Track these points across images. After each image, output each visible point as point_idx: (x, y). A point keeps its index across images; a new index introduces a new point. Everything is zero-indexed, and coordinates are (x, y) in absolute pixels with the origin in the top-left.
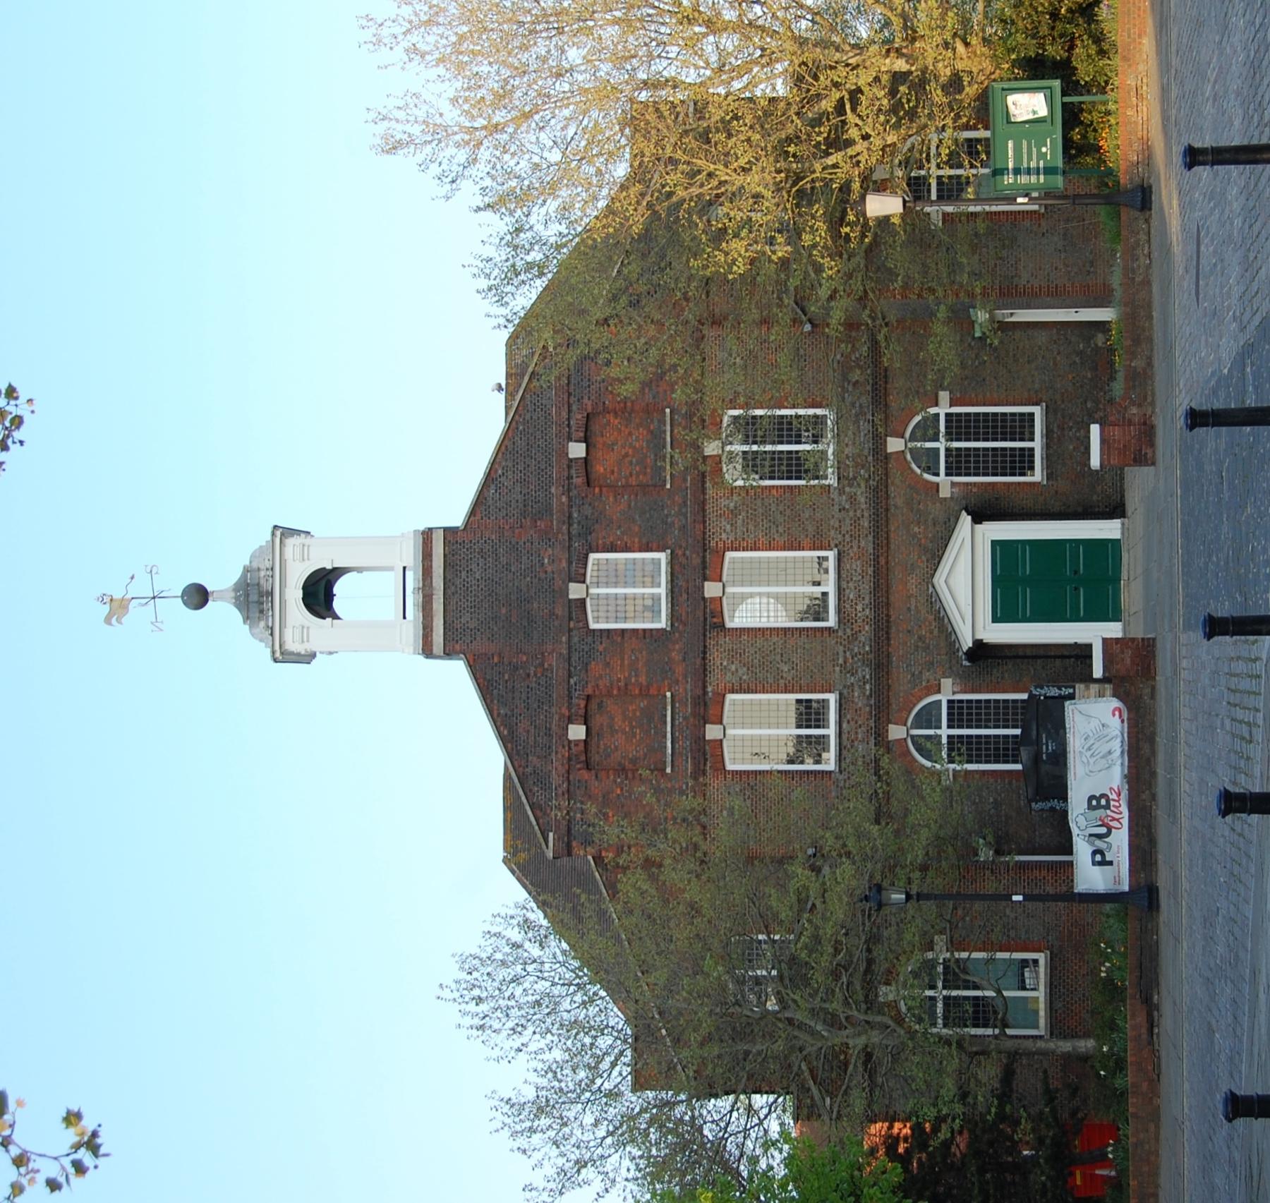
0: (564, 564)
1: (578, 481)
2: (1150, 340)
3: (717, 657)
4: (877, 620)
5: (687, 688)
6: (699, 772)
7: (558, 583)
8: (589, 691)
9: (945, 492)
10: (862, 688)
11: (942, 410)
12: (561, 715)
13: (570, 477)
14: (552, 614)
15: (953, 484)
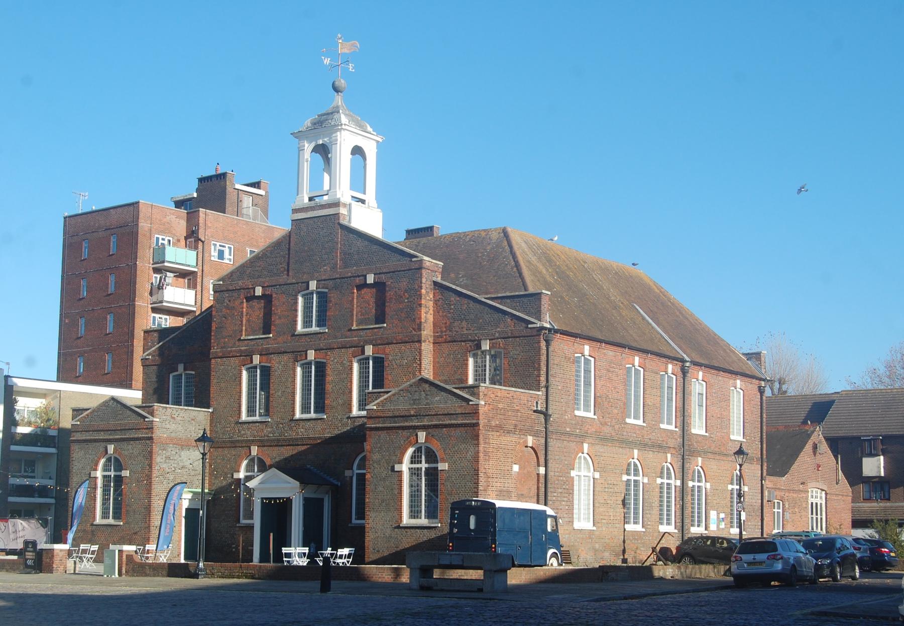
0: (324, 278)
1: (358, 281)
2: (154, 576)
3: (285, 357)
4: (297, 439)
5: (272, 346)
6: (242, 354)
7: (316, 275)
8: (274, 296)
9: (348, 473)
10: (270, 433)
11: (443, 466)
12: (264, 283)
13: (359, 276)
14: (304, 273)
15: (351, 478)
